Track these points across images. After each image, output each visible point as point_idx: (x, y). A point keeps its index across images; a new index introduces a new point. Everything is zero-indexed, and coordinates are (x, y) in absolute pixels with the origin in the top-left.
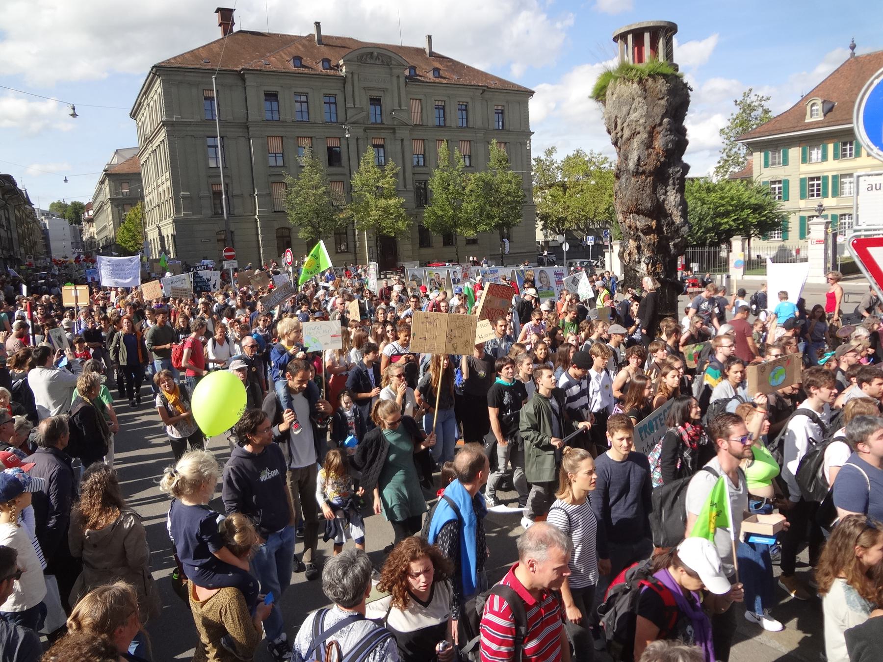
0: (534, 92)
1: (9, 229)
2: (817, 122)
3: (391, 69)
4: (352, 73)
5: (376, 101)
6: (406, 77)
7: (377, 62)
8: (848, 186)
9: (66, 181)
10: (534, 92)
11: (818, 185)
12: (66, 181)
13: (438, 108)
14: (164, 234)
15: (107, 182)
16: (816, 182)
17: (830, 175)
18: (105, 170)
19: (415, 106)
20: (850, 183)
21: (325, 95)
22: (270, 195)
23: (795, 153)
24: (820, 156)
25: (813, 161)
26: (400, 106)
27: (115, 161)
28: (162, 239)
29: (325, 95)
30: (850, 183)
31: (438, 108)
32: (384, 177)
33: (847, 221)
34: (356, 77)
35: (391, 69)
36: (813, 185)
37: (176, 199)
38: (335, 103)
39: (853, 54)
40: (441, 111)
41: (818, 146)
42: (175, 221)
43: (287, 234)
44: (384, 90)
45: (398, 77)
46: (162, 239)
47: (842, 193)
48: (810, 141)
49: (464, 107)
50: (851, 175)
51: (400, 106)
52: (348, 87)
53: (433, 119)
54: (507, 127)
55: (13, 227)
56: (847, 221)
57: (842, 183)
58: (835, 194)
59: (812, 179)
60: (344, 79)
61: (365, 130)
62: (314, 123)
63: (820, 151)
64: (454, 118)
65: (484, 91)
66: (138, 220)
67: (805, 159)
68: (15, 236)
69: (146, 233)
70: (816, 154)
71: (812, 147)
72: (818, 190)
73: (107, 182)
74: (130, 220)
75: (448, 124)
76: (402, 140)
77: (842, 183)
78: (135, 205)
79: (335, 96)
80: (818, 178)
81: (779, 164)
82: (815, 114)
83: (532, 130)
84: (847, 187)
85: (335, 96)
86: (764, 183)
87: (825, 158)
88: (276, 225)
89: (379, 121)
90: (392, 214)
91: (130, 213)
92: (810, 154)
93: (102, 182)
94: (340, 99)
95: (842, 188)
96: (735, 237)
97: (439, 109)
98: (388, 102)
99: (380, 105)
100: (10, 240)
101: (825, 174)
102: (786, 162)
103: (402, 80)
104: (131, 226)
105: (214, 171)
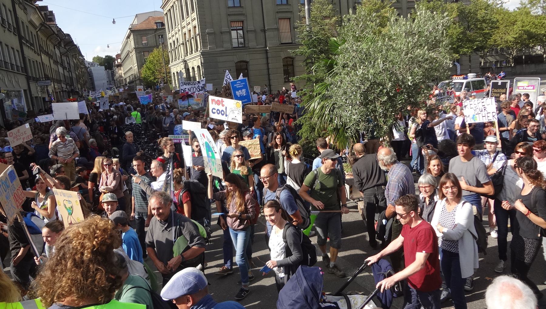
1: (70, 71)
9: (114, 22)
12: (114, 22)
14: (190, 66)
15: (132, 37)
18: (130, 29)
22: (278, 29)
27: (136, 22)
28: (187, 70)
32: (384, 7)
37: (203, 35)
42: (203, 54)
43: (291, 63)
46: (187, 70)
55: (72, 69)
66: (155, 62)
68: (74, 76)
69: (170, 69)
73: (132, 37)
74: (150, 62)
78: (152, 51)
88: (283, 55)
91: (153, 56)
93: (128, 37)
100: (71, 78)
104: (151, 66)
105: (231, 10)
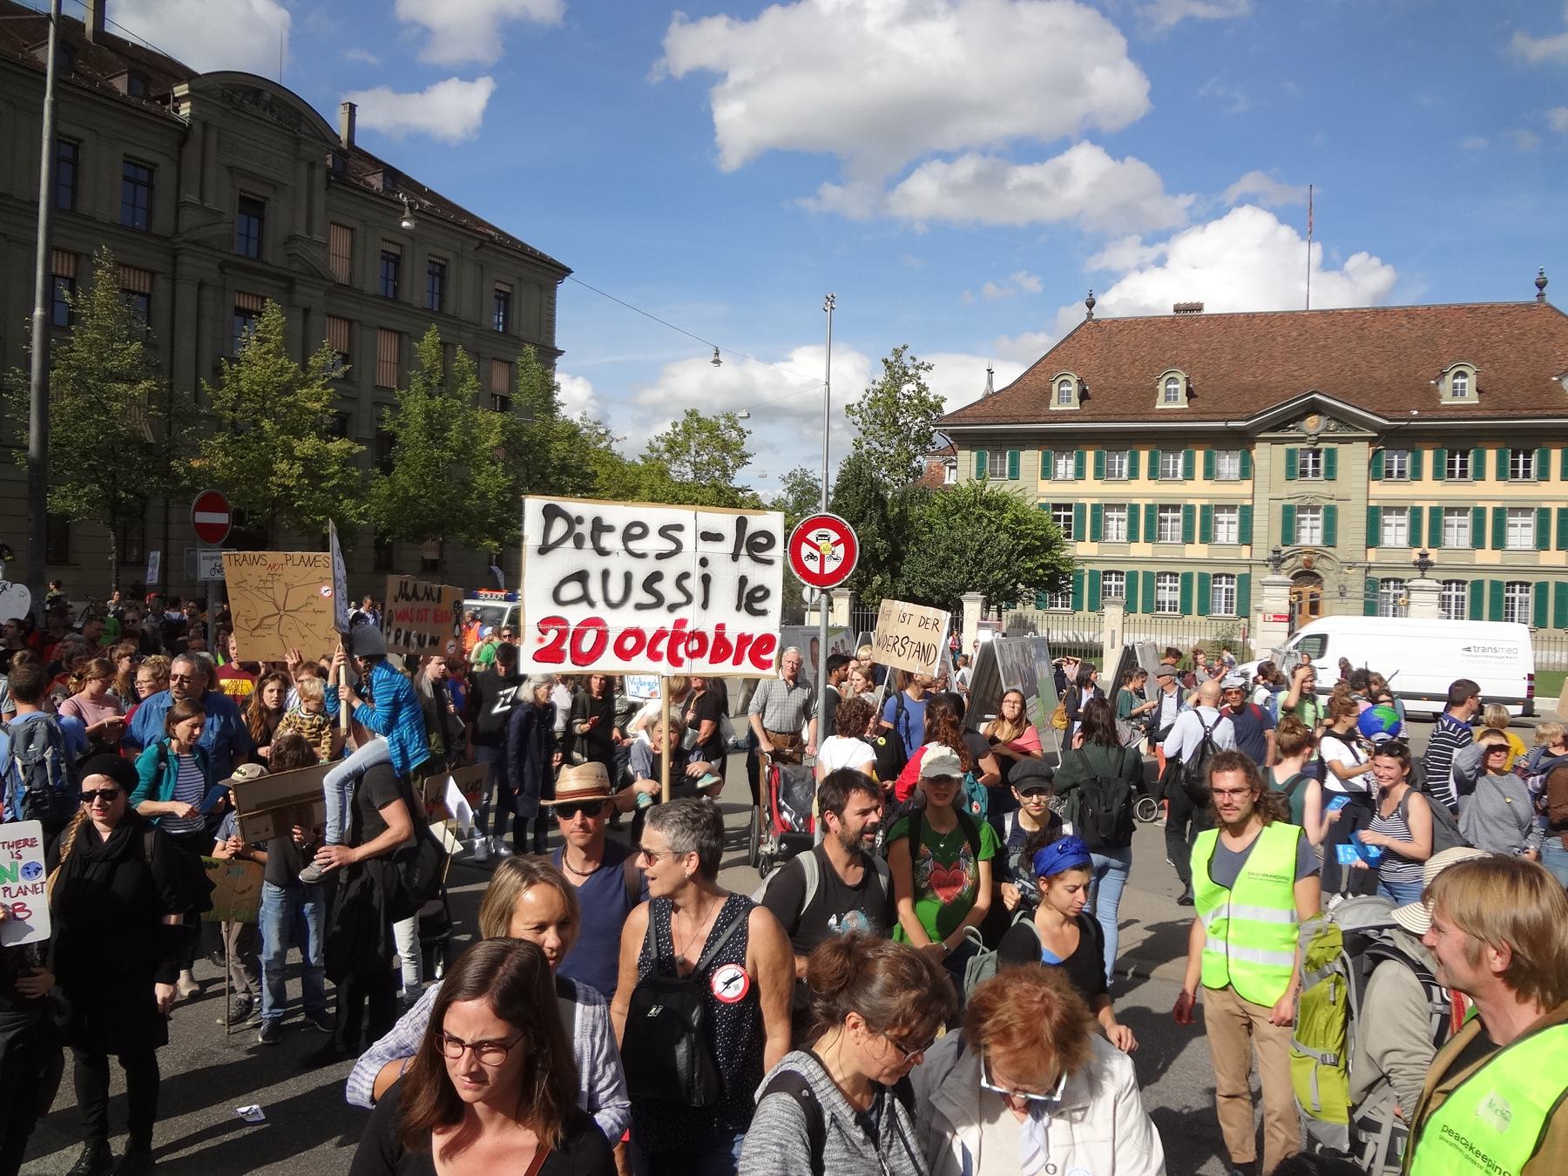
0: (568, 271)
2: (1073, 413)
3: (298, 141)
4: (205, 126)
5: (253, 207)
6: (329, 172)
7: (267, 115)
8: (1117, 526)
10: (569, 271)
11: (1068, 518)
13: (387, 257)
16: (1063, 513)
17: (1089, 502)
19: (340, 241)
20: (1174, 520)
21: (129, 160)
23: (1030, 459)
24: (1071, 469)
25: (1060, 477)
26: (309, 232)
29: (129, 160)
30: (1174, 520)
31: (387, 257)
33: (1113, 583)
34: (213, 138)
35: (298, 141)
36: (1057, 518)
38: (150, 186)
39: (1090, 315)
40: (391, 265)
41: (1176, 451)
44: (276, 186)
45: (312, 165)
47: (1106, 536)
48: (1057, 442)
49: (437, 269)
50: (1176, 508)
51: (309, 232)
52: (192, 152)
53: (373, 281)
54: (514, 331)
56: (1113, 583)
57: (1107, 519)
58: (1097, 536)
59: (1057, 507)
60: (182, 133)
61: (221, 268)
62: (91, 219)
63: (1071, 462)
64: (417, 288)
65: (482, 243)
67: (1047, 473)
70: (1065, 466)
71: (1167, 450)
72: (1068, 527)
75: (405, 294)
76: (307, 311)
77: (1107, 519)
79: (151, 169)
80: (1068, 507)
81: (1003, 475)
82: (1064, 399)
83: (559, 345)
84: (1113, 524)
85: (151, 169)
86: (1043, 506)
87: (1080, 474)
89: (253, 253)
90: (332, 477)
92: (1056, 465)
94: (165, 177)
95: (1106, 527)
96: (969, 595)
97: (388, 260)
98: (282, 217)
99: (261, 219)
101: (1081, 501)
102: (1014, 474)
103: (320, 175)
